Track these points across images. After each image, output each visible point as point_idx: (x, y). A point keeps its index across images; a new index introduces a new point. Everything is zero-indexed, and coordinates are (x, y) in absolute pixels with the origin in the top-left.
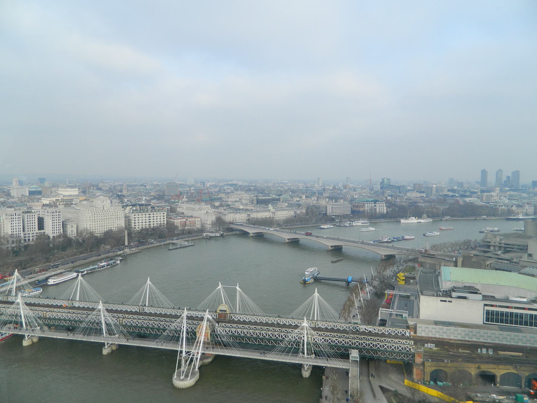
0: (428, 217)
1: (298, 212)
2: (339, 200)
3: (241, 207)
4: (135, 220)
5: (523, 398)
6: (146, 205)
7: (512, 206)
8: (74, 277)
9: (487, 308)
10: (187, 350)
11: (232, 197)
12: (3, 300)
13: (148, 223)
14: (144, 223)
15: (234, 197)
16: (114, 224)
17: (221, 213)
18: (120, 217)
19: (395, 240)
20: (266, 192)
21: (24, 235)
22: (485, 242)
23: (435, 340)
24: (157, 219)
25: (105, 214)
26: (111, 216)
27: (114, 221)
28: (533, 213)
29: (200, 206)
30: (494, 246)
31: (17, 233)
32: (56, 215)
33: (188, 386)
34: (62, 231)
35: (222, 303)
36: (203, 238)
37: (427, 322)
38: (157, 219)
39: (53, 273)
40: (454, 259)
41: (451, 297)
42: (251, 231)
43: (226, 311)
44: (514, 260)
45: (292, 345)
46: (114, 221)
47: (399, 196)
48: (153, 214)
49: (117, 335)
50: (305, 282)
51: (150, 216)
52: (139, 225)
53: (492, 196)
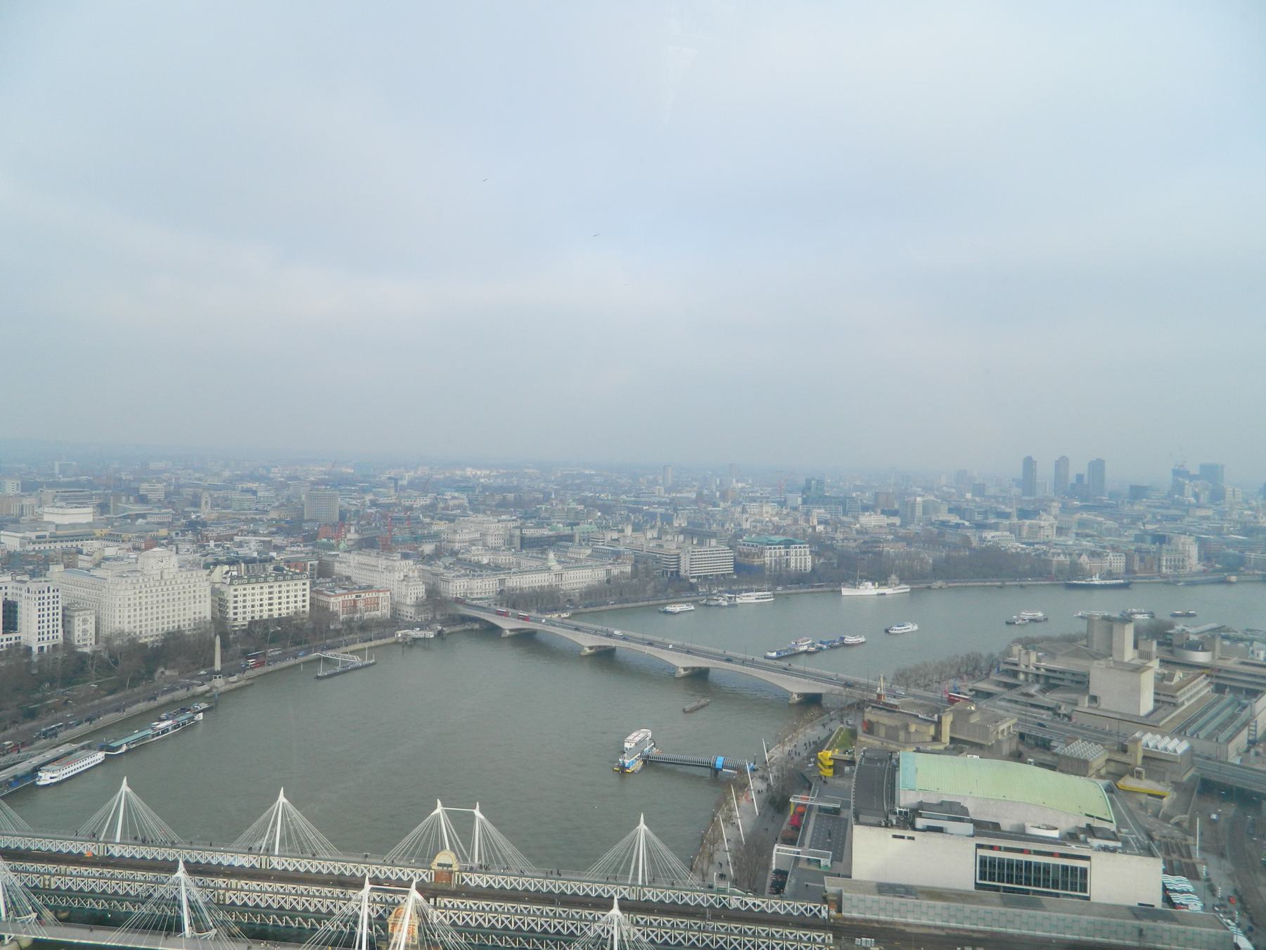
0: (903, 580)
2: (708, 540)
3: (485, 561)
4: (236, 602)
6: (265, 561)
7: (1080, 555)
9: (982, 852)
11: (464, 531)
15: (467, 531)
16: (187, 612)
18: (200, 596)
19: (825, 647)
20: (543, 515)
22: (1007, 663)
23: (876, 925)
24: (288, 597)
25: (165, 589)
26: (179, 593)
28: (1122, 570)
29: (390, 563)
30: (1026, 674)
34: (60, 633)
35: (443, 848)
36: (396, 643)
37: (863, 887)
38: (288, 597)
39: (49, 755)
40: (936, 716)
41: (914, 829)
42: (508, 625)
43: (451, 866)
44: (1062, 708)
46: (187, 606)
47: (842, 523)
49: (214, 931)
51: (271, 590)
52: (244, 613)
53: (1040, 527)
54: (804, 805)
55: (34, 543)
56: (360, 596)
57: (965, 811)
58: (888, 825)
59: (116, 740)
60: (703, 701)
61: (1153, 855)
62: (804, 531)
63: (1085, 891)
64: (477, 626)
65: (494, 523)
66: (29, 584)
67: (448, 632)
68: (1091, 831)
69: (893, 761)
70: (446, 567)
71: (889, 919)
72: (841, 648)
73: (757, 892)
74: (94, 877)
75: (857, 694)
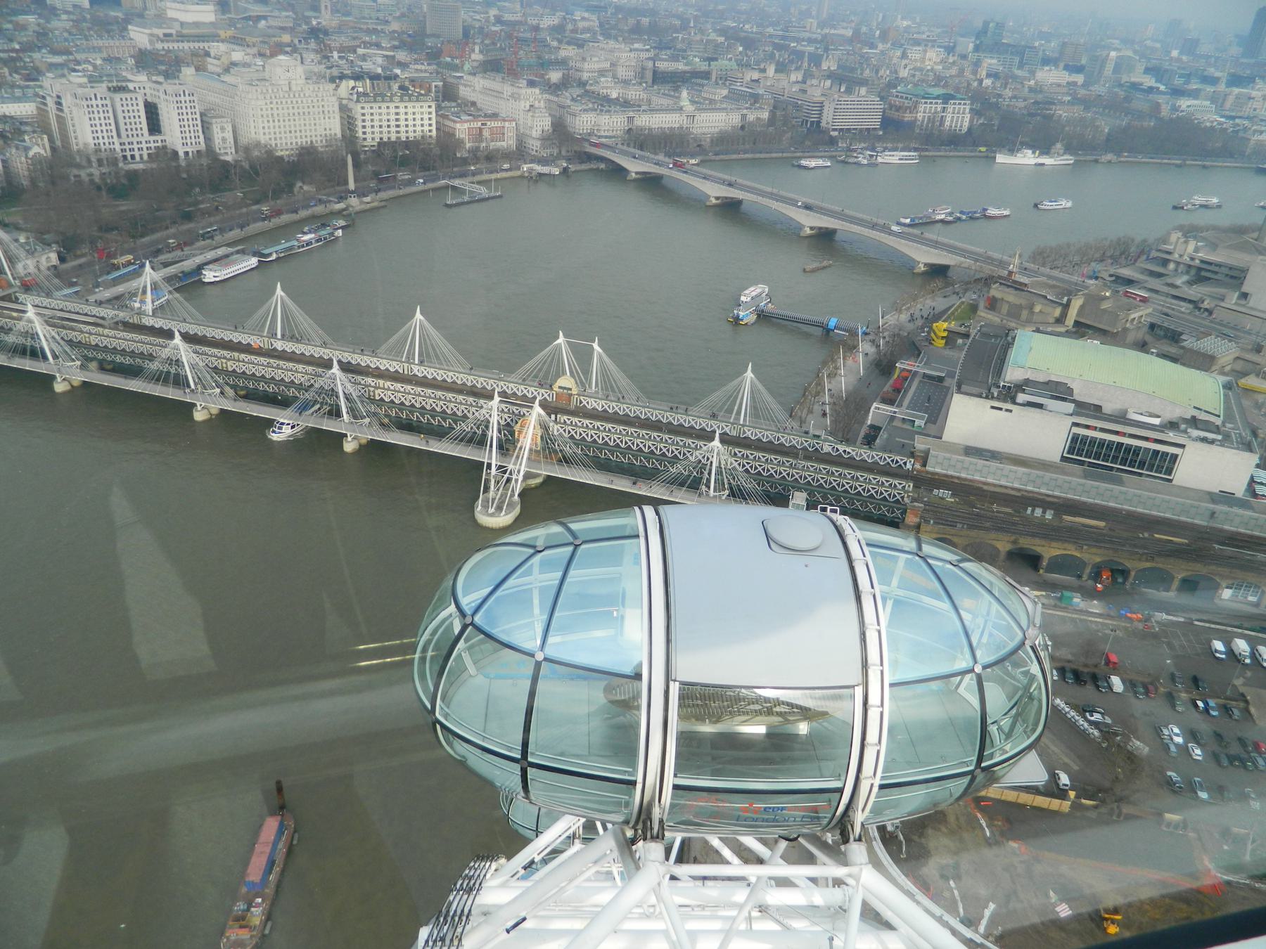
0: (1069, 149)
1: (751, 117)
3: (614, 95)
5: (1071, 598)
6: (388, 78)
8: (253, 266)
9: (1076, 430)
10: (499, 464)
12: (131, 321)
13: (393, 129)
14: (385, 129)
16: (318, 127)
17: (563, 107)
18: (329, 112)
19: (964, 217)
20: (679, 46)
21: (121, 144)
22: (1160, 250)
23: (956, 481)
27: (317, 122)
29: (516, 90)
30: (1178, 263)
31: (106, 141)
32: (185, 102)
33: (501, 525)
34: (202, 139)
35: (564, 373)
36: (522, 177)
37: (951, 448)
38: (414, 119)
39: (210, 255)
40: (1066, 299)
41: (1014, 402)
42: (634, 167)
43: (571, 389)
44: (1206, 303)
45: (690, 471)
47: (1014, 77)
48: (406, 107)
49: (367, 420)
50: (737, 319)
51: (397, 111)
53: (1250, 98)
54: (908, 371)
55: (162, 41)
56: (486, 124)
57: (1070, 391)
58: (989, 396)
59: (266, 247)
60: (825, 263)
61: (1251, 451)
62: (969, 84)
63: (1170, 474)
64: (602, 166)
65: (626, 52)
66: (165, 86)
67: (573, 170)
68: (1194, 422)
69: (1009, 338)
70: (573, 100)
71: (969, 477)
72: (981, 220)
73: (848, 441)
74: (263, 365)
75: (988, 269)
